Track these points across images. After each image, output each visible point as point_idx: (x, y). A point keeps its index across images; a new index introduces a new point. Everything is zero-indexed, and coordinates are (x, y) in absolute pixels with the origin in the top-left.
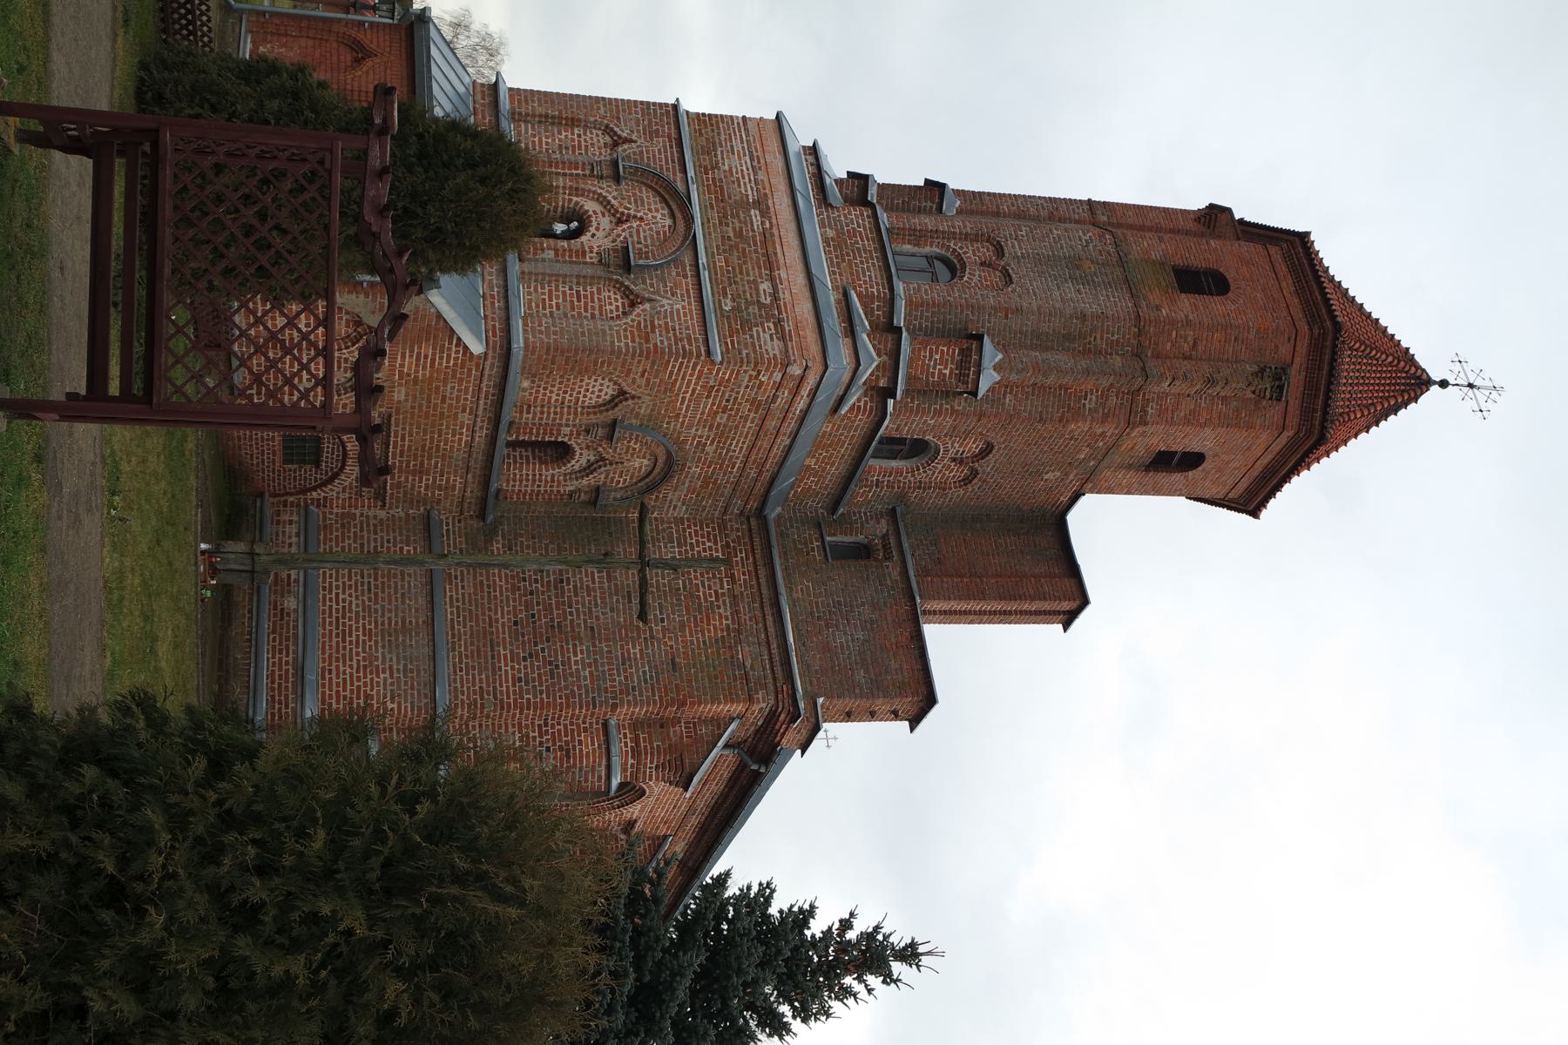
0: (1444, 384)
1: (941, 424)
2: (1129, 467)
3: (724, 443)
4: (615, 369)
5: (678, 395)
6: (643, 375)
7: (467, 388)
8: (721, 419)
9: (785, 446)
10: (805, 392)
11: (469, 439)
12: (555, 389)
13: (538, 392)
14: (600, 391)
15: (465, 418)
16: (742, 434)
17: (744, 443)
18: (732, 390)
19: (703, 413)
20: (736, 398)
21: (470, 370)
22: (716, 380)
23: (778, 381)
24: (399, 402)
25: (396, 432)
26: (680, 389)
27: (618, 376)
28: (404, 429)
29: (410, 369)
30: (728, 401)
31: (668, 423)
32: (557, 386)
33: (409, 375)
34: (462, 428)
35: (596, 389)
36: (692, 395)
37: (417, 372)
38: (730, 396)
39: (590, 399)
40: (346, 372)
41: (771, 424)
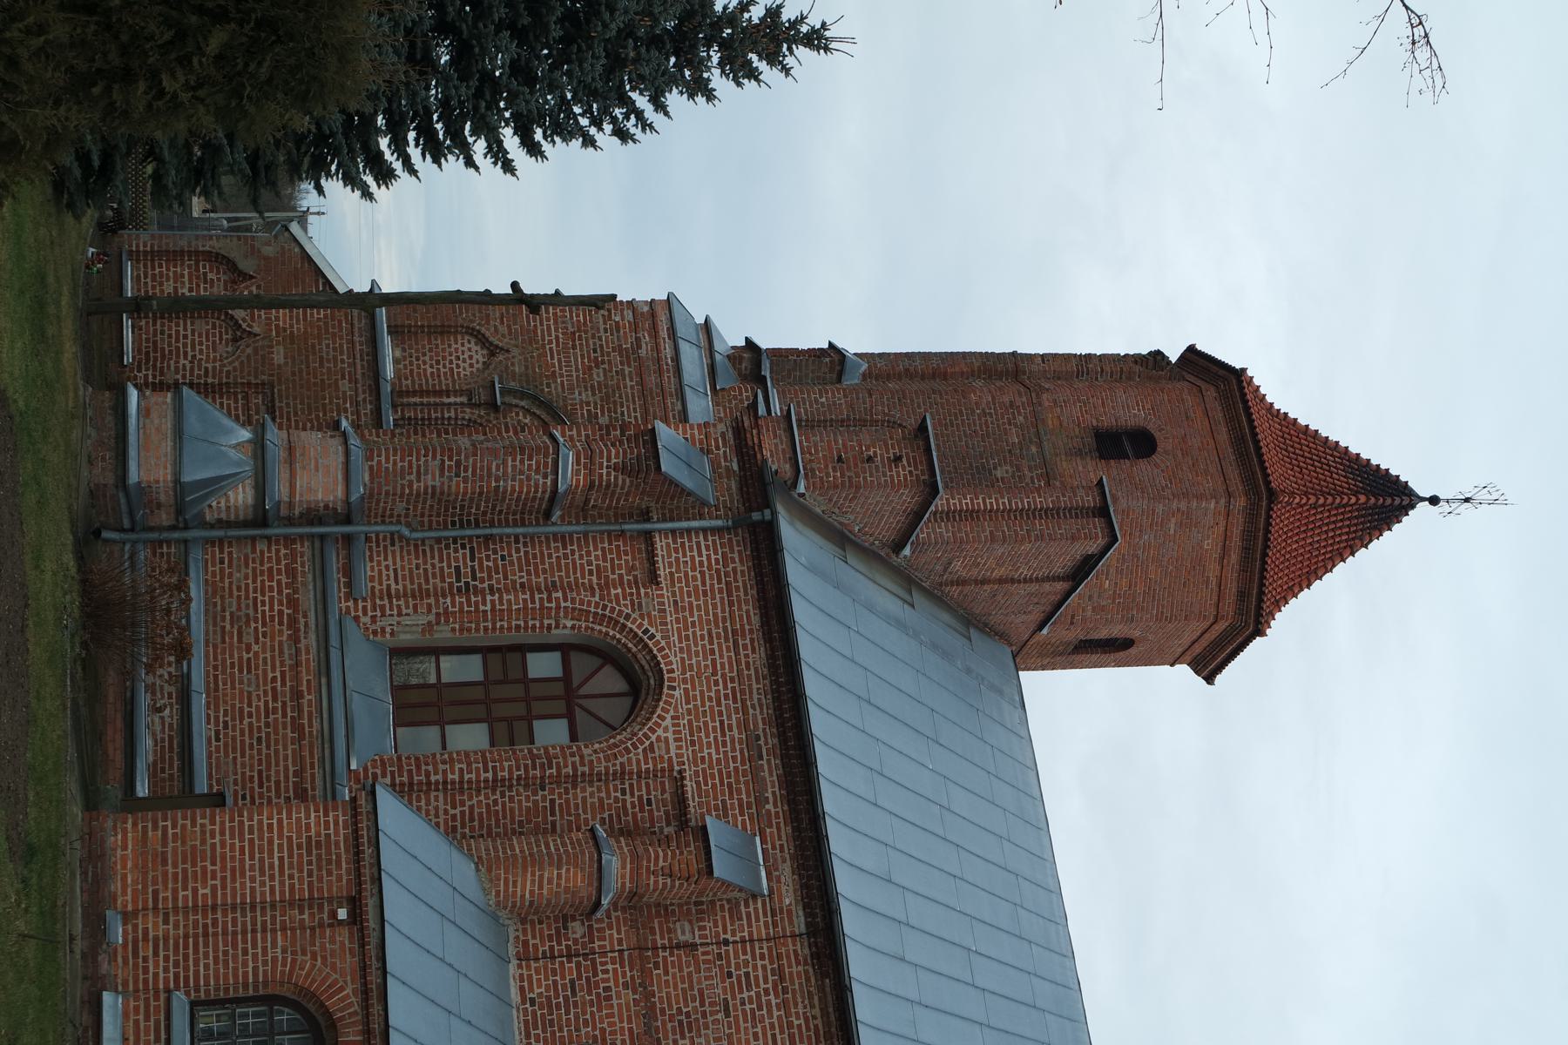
0: (1434, 500)
1: (834, 403)
2: (1080, 453)
3: (616, 413)
4: (474, 315)
5: (544, 346)
6: (502, 323)
7: (341, 345)
8: (598, 376)
9: (679, 412)
10: (664, 333)
11: (355, 417)
12: (427, 358)
13: (411, 364)
14: (471, 357)
15: (345, 385)
16: (627, 396)
17: (635, 410)
18: (593, 337)
19: (577, 370)
20: (601, 346)
21: (340, 322)
22: (573, 323)
23: (632, 320)
24: (279, 366)
25: (281, 408)
26: (543, 340)
27: (479, 324)
28: (288, 405)
29: (285, 322)
30: (595, 351)
31: (548, 385)
32: (428, 354)
33: (285, 330)
34: (345, 402)
35: (466, 356)
36: (558, 345)
37: (291, 326)
38: (595, 344)
39: (464, 369)
40: (227, 345)
41: (652, 380)
